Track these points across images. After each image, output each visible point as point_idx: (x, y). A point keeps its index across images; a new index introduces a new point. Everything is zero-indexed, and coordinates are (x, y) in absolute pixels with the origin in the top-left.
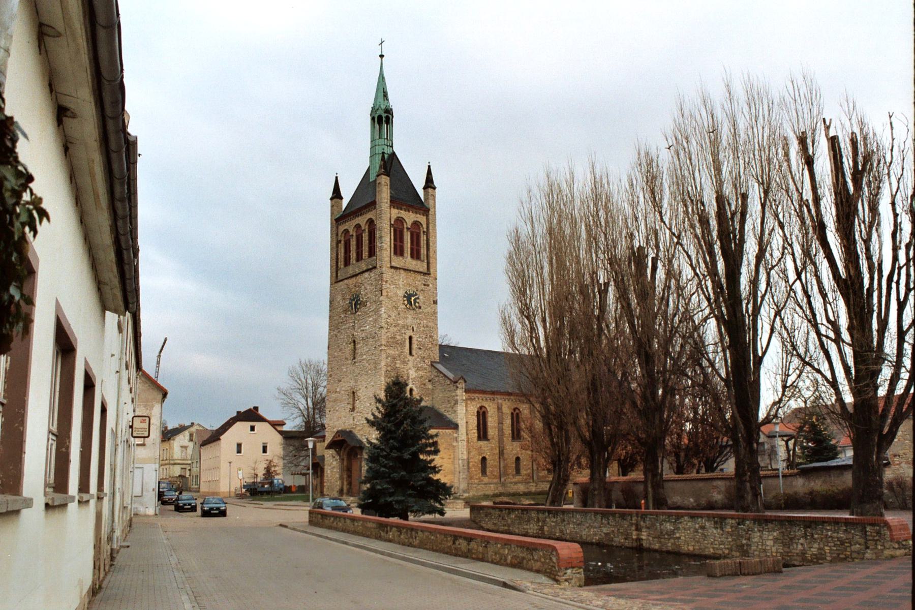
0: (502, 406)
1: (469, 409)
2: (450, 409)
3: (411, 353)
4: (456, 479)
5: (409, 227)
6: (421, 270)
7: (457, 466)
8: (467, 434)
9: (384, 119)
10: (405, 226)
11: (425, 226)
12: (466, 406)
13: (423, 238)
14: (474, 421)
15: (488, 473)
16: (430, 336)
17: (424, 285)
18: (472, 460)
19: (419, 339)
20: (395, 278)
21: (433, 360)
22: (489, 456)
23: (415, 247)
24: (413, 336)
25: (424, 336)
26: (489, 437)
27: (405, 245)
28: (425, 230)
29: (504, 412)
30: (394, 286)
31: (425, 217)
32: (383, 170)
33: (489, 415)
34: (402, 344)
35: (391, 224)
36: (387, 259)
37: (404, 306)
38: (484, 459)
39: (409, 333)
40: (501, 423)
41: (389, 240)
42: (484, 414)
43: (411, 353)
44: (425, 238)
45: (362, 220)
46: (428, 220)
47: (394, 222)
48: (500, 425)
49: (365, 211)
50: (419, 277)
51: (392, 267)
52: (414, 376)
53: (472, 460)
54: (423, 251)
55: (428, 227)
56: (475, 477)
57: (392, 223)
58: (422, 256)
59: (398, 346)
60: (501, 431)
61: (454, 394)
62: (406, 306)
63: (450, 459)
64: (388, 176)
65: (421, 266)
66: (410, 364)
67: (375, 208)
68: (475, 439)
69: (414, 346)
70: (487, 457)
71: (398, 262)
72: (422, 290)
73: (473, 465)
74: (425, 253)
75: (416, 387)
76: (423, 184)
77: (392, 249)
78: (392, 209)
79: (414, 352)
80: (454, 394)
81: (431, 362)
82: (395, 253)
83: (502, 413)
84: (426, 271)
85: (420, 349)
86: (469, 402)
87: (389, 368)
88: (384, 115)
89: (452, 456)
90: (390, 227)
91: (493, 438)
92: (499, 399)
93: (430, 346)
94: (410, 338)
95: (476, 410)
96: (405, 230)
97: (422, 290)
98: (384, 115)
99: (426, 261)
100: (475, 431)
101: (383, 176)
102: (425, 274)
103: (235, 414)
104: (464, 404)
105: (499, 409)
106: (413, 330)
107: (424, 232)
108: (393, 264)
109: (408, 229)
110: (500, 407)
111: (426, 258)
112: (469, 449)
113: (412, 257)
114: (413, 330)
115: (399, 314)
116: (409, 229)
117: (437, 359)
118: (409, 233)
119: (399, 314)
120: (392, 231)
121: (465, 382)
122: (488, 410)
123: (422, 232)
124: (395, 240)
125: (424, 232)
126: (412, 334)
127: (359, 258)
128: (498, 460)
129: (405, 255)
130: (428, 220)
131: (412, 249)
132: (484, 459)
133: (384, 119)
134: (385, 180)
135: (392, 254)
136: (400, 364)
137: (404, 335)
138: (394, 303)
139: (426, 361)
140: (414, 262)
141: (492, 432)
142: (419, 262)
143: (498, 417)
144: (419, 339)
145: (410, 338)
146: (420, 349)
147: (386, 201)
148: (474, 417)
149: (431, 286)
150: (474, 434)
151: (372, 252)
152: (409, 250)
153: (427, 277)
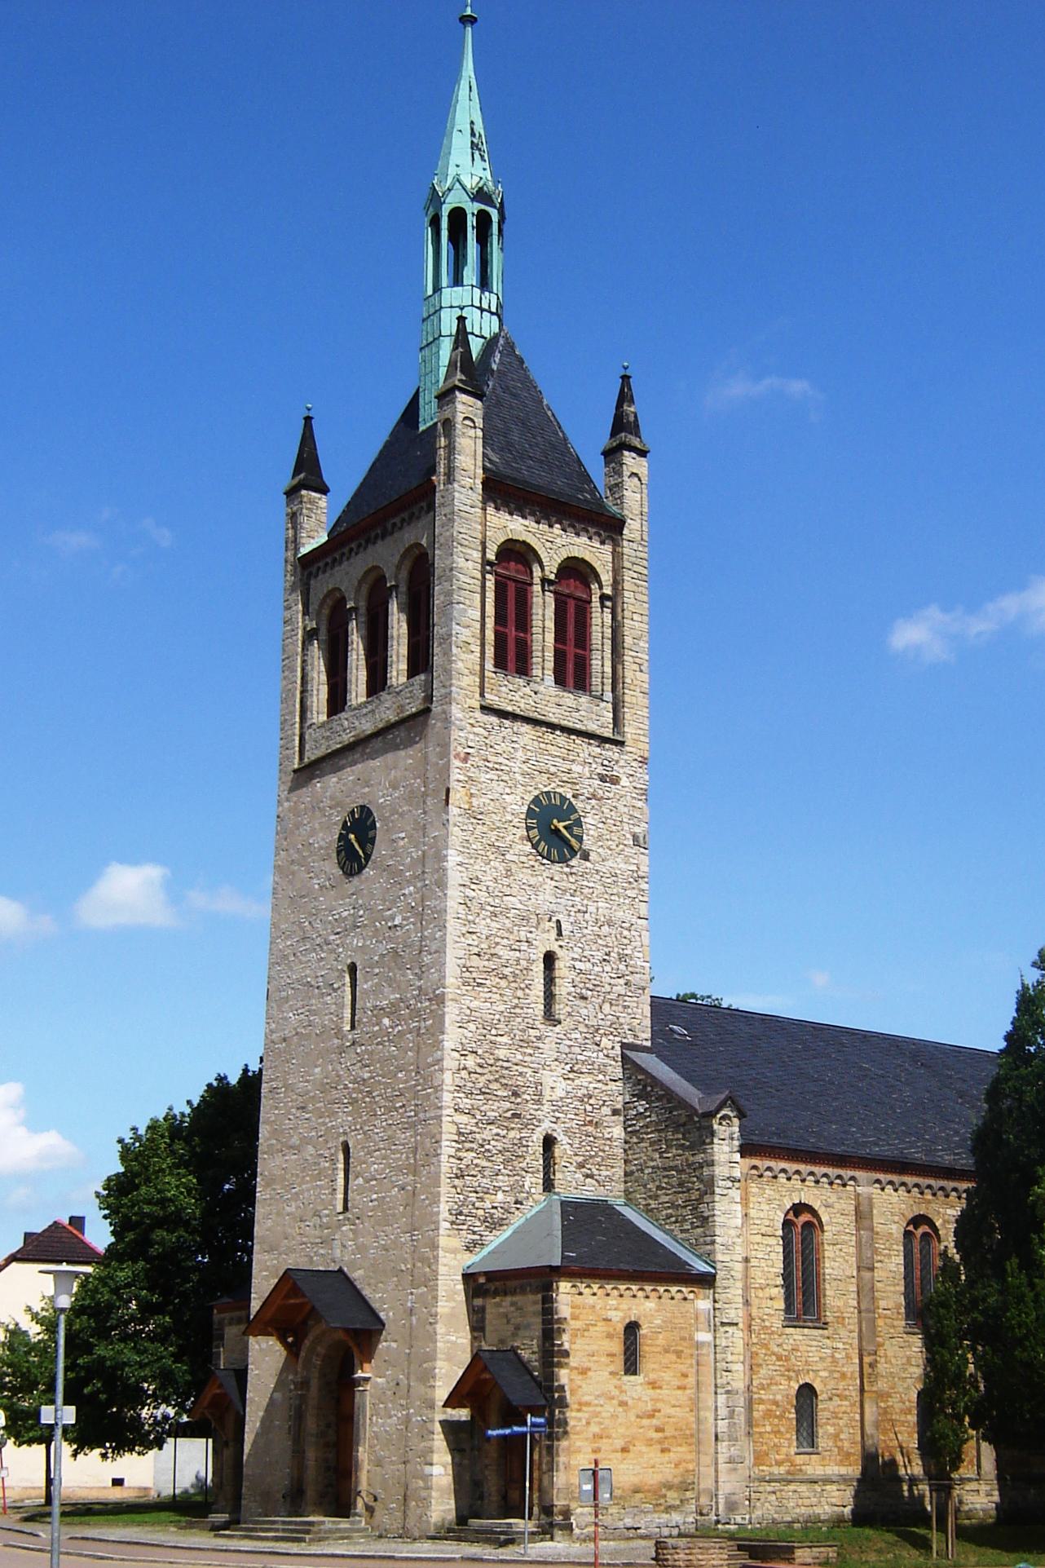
0: (871, 1206)
1: (753, 1213)
2: (687, 1212)
3: (550, 1017)
4: (706, 1460)
5: (552, 577)
6: (592, 727)
7: (709, 1416)
8: (747, 1303)
9: (471, 221)
10: (537, 572)
11: (606, 577)
12: (745, 1201)
13: (600, 621)
14: (770, 1260)
15: (822, 1442)
16: (622, 958)
17: (603, 779)
18: (763, 1395)
19: (578, 965)
20: (499, 749)
21: (630, 1040)
22: (824, 1381)
23: (571, 650)
24: (560, 953)
25: (600, 955)
26: (829, 1316)
27: (537, 638)
28: (608, 591)
29: (878, 1228)
30: (492, 775)
31: (608, 548)
32: (459, 376)
33: (827, 1236)
34: (518, 978)
35: (485, 562)
36: (470, 681)
37: (528, 848)
38: (807, 1393)
39: (546, 941)
40: (865, 1266)
41: (477, 615)
42: (814, 1226)
43: (550, 1017)
44: (608, 618)
45: (387, 555)
46: (617, 556)
47: (497, 555)
48: (867, 1275)
49: (397, 520)
50: (585, 749)
51: (486, 709)
52: (560, 1093)
53: (763, 1395)
54: (600, 663)
55: (617, 583)
56: (774, 1456)
57: (491, 556)
58: (596, 681)
59: (503, 983)
60: (866, 1293)
61: (699, 1158)
62: (535, 846)
63: (682, 1388)
64: (479, 396)
65: (595, 715)
66: (548, 1049)
67: (431, 507)
68: (777, 1321)
69: (562, 989)
70: (817, 1386)
71: (510, 692)
72: (594, 796)
73: (768, 1414)
74: (608, 669)
75: (566, 1132)
76: (604, 440)
77: (490, 652)
78: (490, 510)
79: (560, 1009)
80: (699, 1158)
81: (624, 1046)
82: (500, 663)
83: (872, 1229)
84: (608, 733)
85: (584, 998)
86: (754, 1188)
87: (471, 1062)
88: (472, 208)
89: (691, 1380)
90: (483, 573)
91: (841, 1320)
92: (865, 1184)
93: (621, 990)
94: (549, 959)
95: (780, 1218)
96: (537, 588)
97: (594, 796)
98: (472, 208)
99: (608, 696)
100: (779, 1292)
101: (461, 397)
102: (603, 740)
103: (303, 421)
104: (736, 1194)
105: (862, 1215)
106: (560, 934)
107: (603, 598)
108: (491, 699)
109: (544, 581)
110: (864, 1208)
111: (608, 688)
112: (753, 1355)
113: (560, 680)
114: (560, 934)
115: (509, 873)
116: (551, 582)
117: (644, 1037)
118: (550, 599)
119: (509, 873)
120: (490, 584)
121: (741, 1115)
122: (825, 1219)
123: (595, 599)
124: (500, 618)
125: (603, 598)
126: (555, 947)
127: (377, 681)
128: (855, 1395)
129: (537, 671)
130: (617, 556)
131: (560, 657)
132: (807, 1393)
133: (471, 221)
134: (466, 406)
135: (489, 665)
136: (509, 1046)
137: (524, 946)
138: (493, 836)
139: (605, 1042)
140: (568, 699)
141: (838, 1295)
142: (584, 699)
143: (859, 1245)
144: (578, 965)
145: (549, 959)
146: (584, 998)
147: (468, 482)
148: (772, 1241)
149: (624, 781)
150: (772, 1301)
151: (420, 660)
152: (550, 655)
153: (611, 752)
